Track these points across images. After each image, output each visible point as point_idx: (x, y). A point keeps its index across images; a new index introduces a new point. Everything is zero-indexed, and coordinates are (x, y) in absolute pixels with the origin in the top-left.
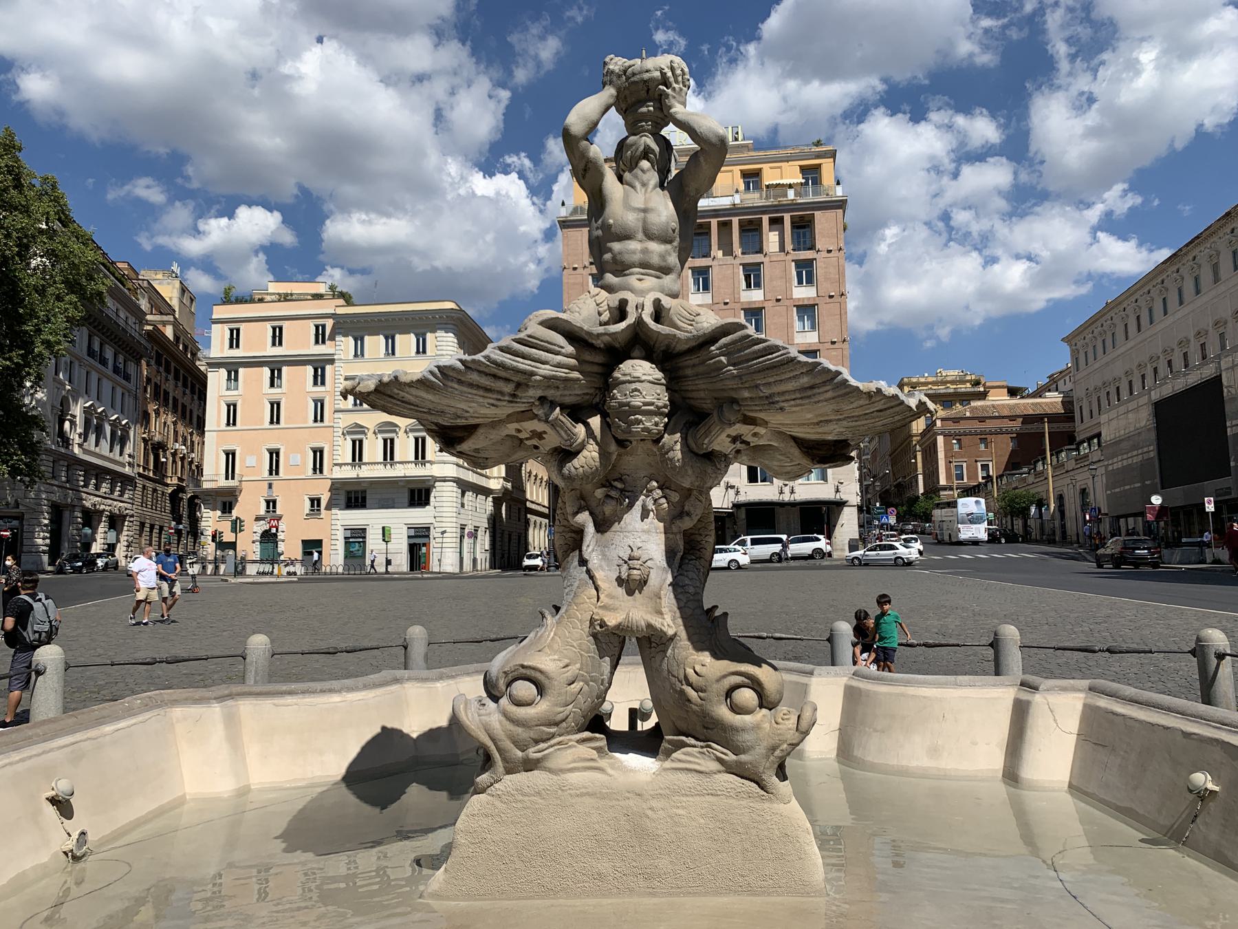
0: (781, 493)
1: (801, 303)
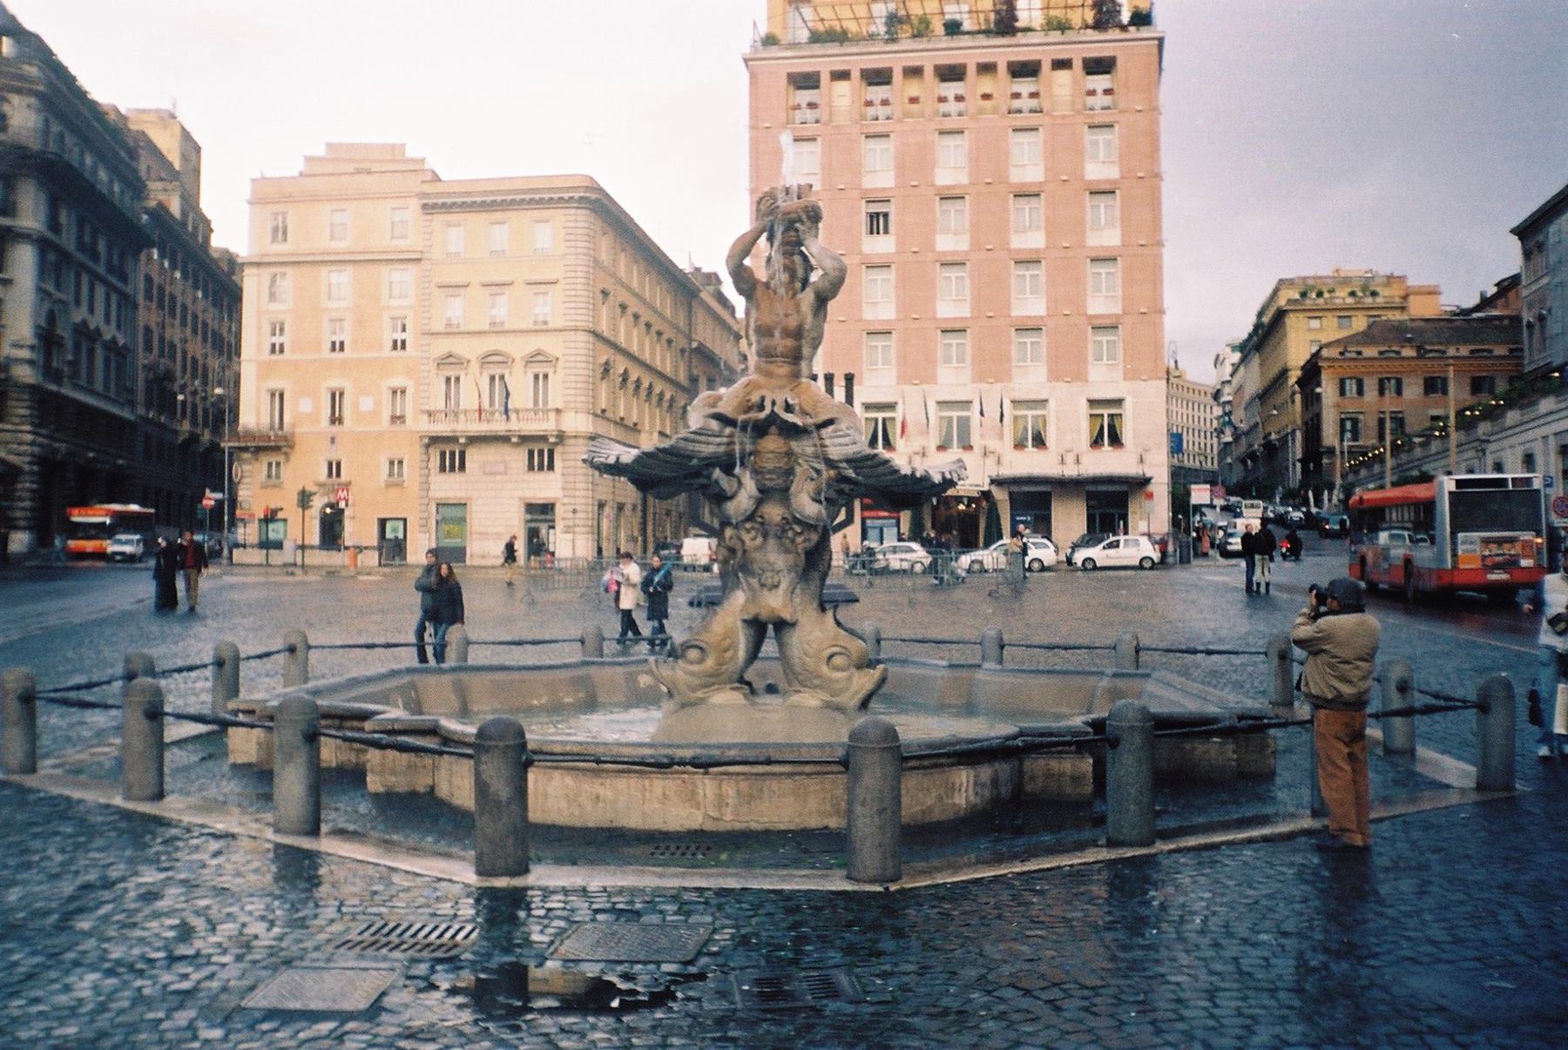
0: (1062, 462)
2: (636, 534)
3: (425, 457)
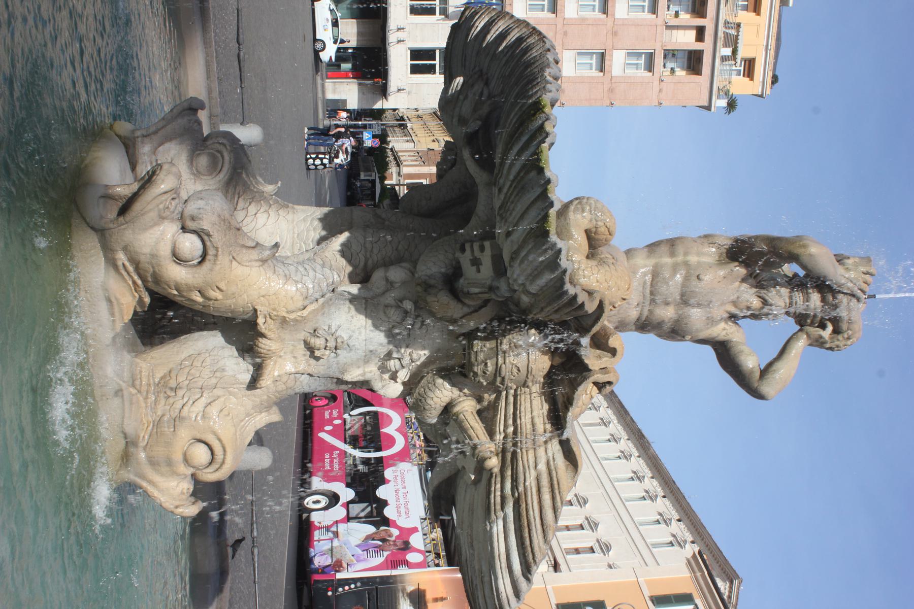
0: (399, 29)
1: (607, 57)
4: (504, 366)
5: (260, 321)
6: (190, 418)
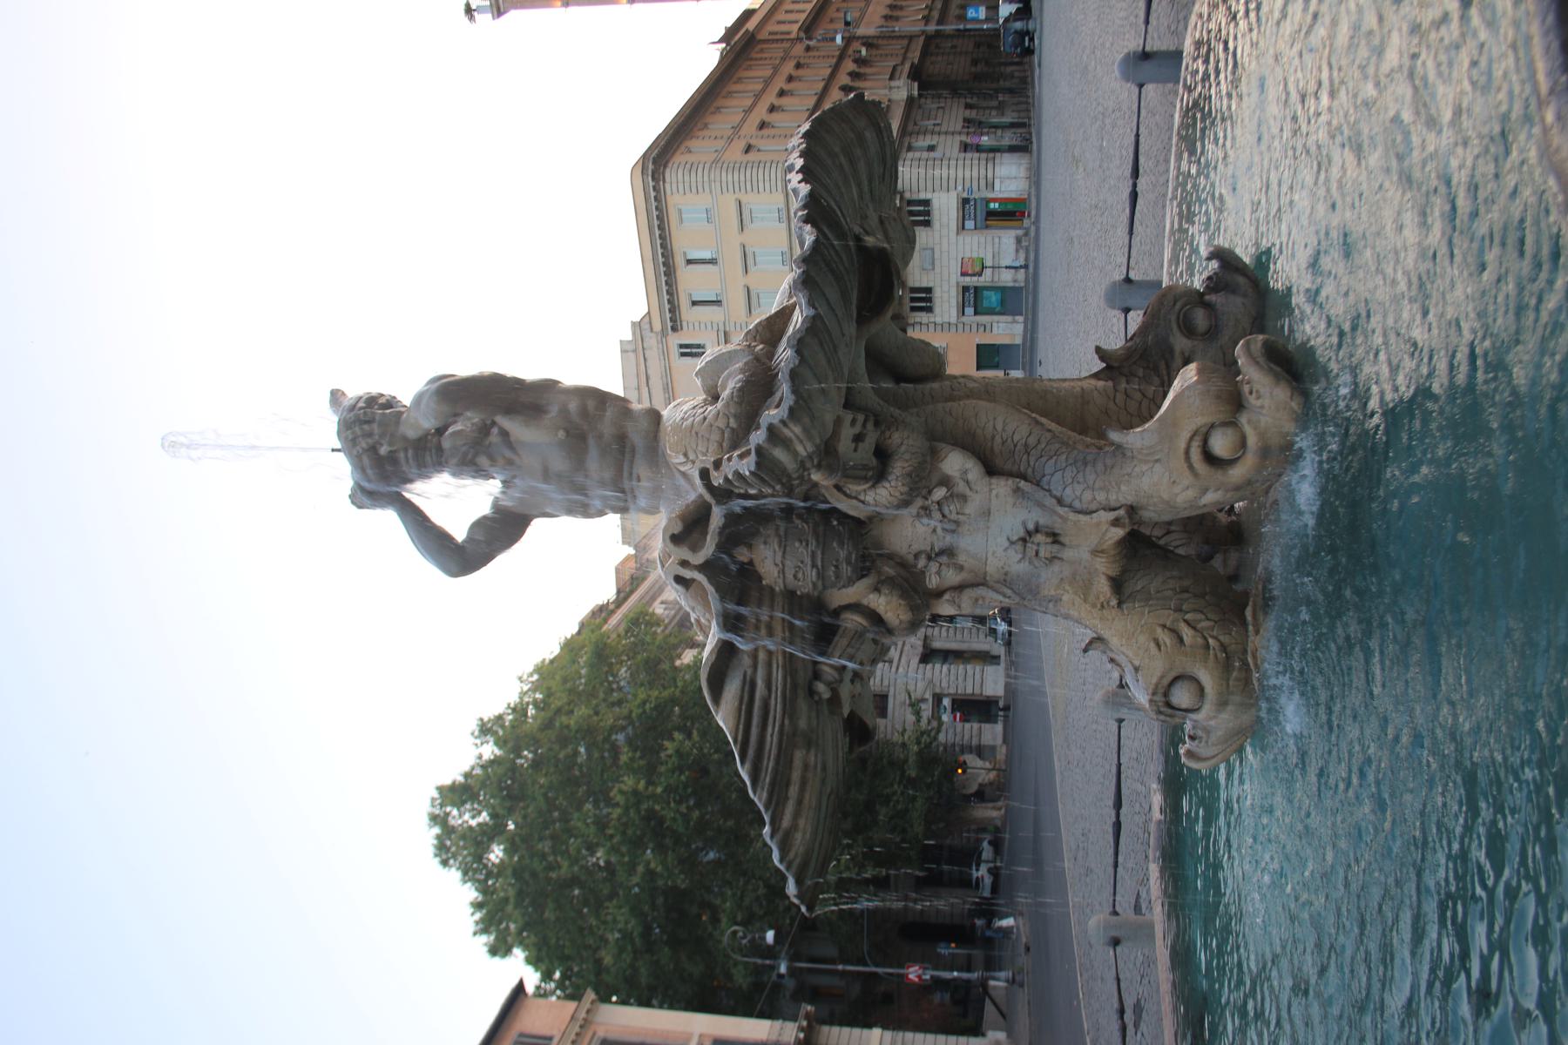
2: (995, 103)
3: (917, 328)
4: (814, 579)
5: (1114, 602)
6: (1227, 491)
